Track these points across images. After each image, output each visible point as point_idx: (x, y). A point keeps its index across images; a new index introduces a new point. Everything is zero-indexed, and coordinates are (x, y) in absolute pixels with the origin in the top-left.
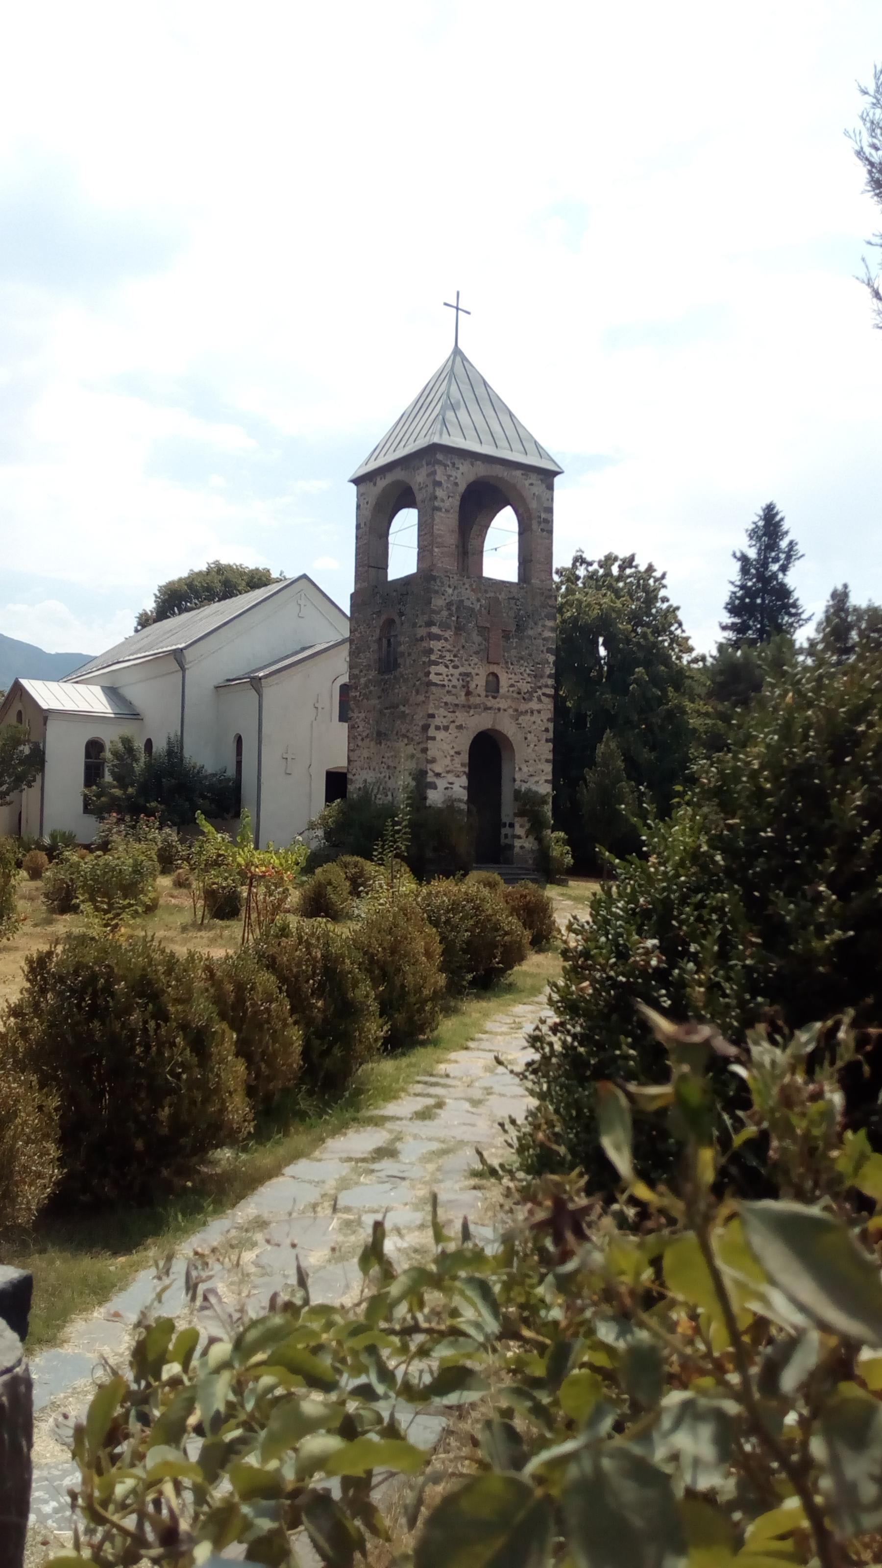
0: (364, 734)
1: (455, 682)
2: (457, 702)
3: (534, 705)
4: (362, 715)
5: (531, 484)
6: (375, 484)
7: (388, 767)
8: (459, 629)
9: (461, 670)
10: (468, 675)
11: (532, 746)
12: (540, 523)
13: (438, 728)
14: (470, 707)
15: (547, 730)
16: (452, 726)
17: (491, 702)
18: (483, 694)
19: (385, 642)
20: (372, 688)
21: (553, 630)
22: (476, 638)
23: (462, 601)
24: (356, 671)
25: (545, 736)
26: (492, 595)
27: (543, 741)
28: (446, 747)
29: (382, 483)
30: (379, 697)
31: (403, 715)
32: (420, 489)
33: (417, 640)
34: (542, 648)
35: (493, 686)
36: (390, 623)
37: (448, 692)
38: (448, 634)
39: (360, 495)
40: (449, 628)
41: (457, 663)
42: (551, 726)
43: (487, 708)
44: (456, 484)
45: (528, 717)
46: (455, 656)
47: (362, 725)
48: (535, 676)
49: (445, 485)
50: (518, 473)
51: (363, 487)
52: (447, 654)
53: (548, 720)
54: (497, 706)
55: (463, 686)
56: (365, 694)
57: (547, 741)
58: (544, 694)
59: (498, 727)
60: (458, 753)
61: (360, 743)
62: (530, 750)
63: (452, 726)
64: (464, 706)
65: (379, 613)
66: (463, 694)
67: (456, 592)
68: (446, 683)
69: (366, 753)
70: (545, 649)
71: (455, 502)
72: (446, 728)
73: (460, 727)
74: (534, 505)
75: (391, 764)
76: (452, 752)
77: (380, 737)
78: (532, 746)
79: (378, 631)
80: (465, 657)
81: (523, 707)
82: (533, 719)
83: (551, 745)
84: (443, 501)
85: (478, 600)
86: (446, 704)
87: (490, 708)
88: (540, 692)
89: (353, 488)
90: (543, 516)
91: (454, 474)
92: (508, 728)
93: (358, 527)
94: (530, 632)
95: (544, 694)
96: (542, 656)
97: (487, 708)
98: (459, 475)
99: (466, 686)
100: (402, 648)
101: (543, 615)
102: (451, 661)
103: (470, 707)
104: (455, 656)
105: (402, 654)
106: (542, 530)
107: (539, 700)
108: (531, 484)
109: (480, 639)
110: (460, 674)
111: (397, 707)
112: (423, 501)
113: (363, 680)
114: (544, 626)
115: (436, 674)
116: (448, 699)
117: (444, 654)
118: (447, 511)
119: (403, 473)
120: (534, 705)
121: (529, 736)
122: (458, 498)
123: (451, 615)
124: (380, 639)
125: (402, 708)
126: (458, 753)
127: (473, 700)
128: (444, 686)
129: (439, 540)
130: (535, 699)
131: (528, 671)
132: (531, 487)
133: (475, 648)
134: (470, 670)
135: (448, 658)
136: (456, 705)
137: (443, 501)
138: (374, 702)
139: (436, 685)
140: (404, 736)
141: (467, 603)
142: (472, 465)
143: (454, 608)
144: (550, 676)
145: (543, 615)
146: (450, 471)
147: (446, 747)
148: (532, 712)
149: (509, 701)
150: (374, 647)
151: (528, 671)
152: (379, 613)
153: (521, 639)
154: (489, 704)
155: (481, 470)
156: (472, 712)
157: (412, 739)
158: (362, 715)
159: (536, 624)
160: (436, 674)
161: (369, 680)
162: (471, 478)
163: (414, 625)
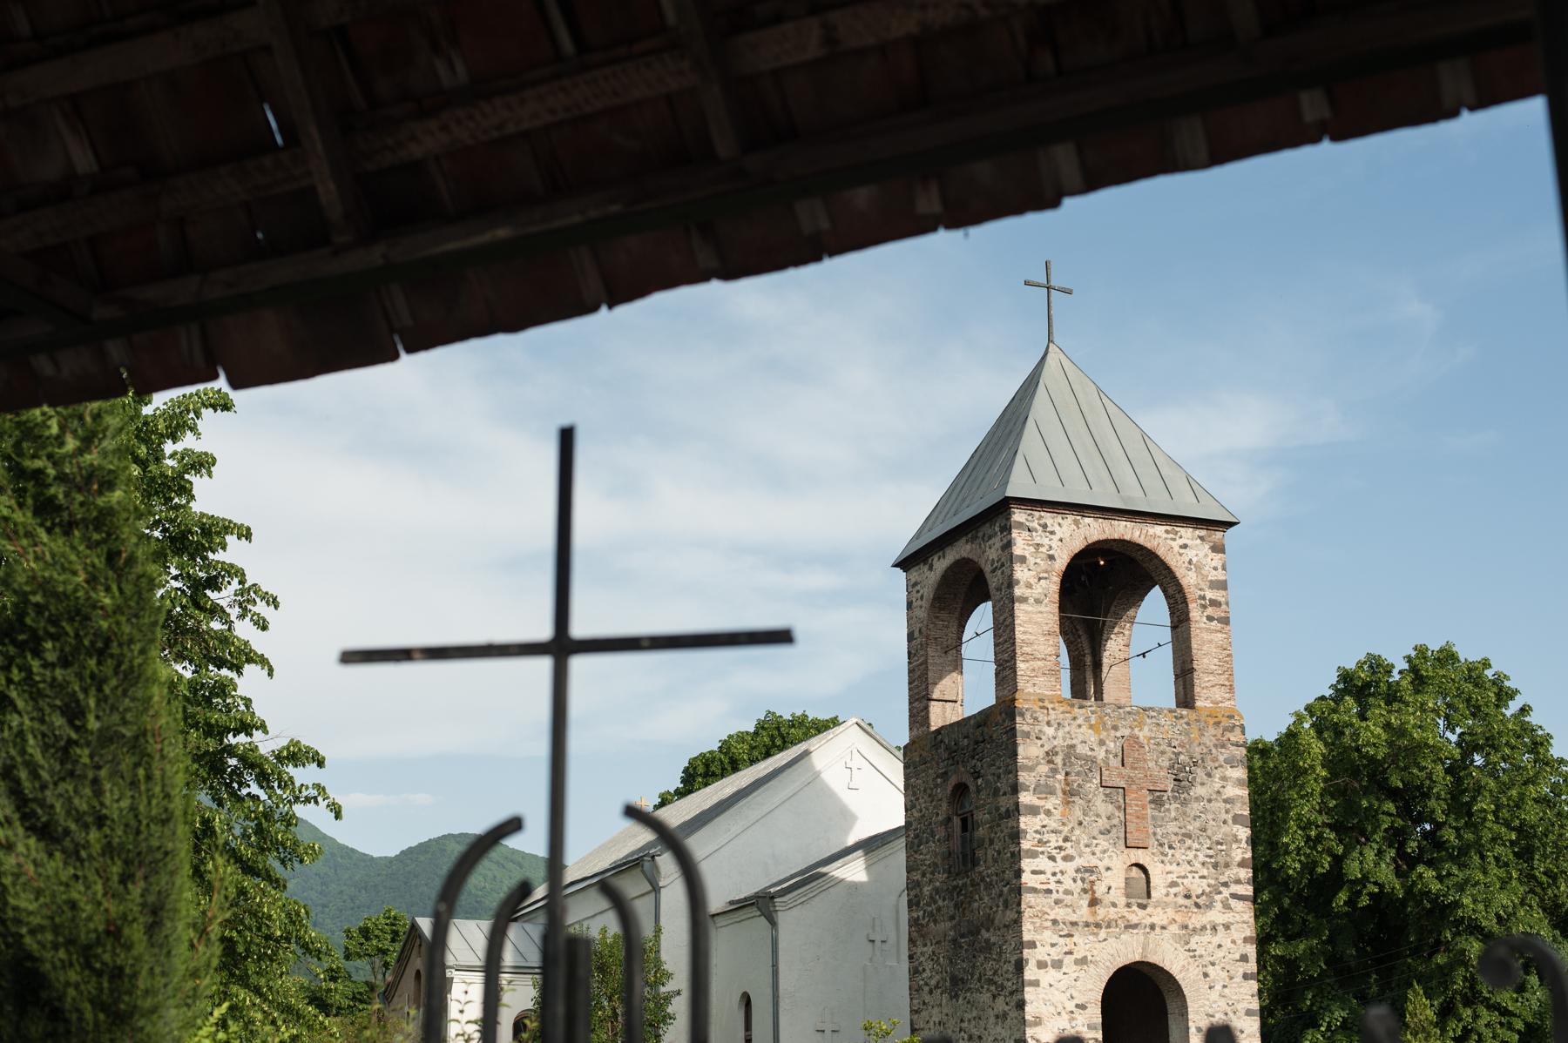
0: (933, 982)
1: (1068, 883)
2: (1074, 918)
3: (1216, 915)
4: (929, 949)
5: (1185, 546)
6: (931, 568)
8: (1070, 794)
9: (1079, 862)
10: (1090, 870)
11: (1218, 987)
12: (1204, 607)
13: (1041, 965)
14: (1098, 926)
15: (1244, 958)
16: (1068, 960)
17: (1136, 915)
18: (1122, 901)
19: (957, 821)
20: (940, 903)
21: (1239, 782)
22: (1101, 806)
23: (1073, 747)
24: (917, 876)
25: (1242, 968)
26: (1127, 732)
27: (1238, 979)
28: (1059, 997)
29: (941, 564)
30: (952, 918)
31: (988, 946)
32: (993, 571)
34: (1224, 816)
35: (1141, 886)
36: (961, 790)
37: (1057, 902)
38: (1052, 803)
39: (912, 586)
40: (1052, 792)
41: (1070, 851)
42: (1251, 950)
43: (1130, 926)
44: (1051, 558)
45: (1207, 937)
46: (1066, 840)
47: (928, 965)
48: (1215, 866)
49: (1031, 560)
50: (1159, 530)
51: (915, 575)
52: (1053, 838)
53: (1246, 940)
54: (1148, 921)
55: (1085, 891)
56: (931, 914)
57: (1246, 977)
58: (1234, 896)
59: (1153, 959)
60: (1082, 1007)
61: (927, 998)
62: (1214, 995)
63: (1068, 960)
64: (1087, 925)
65: (945, 776)
66: (1085, 903)
67: (1060, 733)
68: (1052, 886)
70: (1229, 817)
71: (1053, 586)
72: (1058, 964)
73: (1082, 961)
74: (1188, 579)
75: (975, 1032)
76: (1071, 1006)
77: (956, 985)
78: (1218, 987)
79: (945, 805)
80: (1085, 839)
81: (1197, 920)
82: (1216, 940)
83: (1253, 986)
84: (1029, 586)
85: (1102, 743)
86: (1055, 922)
87: (1135, 926)
88: (1226, 892)
89: (901, 575)
90: (1210, 594)
91: (1046, 541)
92: (1172, 959)
93: (910, 637)
94: (1198, 791)
95: (1234, 896)
96: (1225, 829)
97: (1130, 926)
98: (1055, 544)
99: (1089, 890)
100: (981, 832)
101: (1221, 758)
102: (1060, 848)
103: (1098, 926)
104: (1066, 840)
105: (981, 844)
106: (1210, 619)
107: (1227, 907)
108: (1185, 546)
109: (1110, 807)
110: (1077, 871)
111: (978, 932)
112: (999, 589)
113: (927, 890)
114: (1224, 778)
115: (1034, 872)
116: (1060, 913)
117: (1046, 837)
118: (1038, 601)
119: (968, 547)
120: (1216, 915)
121: (1210, 970)
122: (1057, 580)
123: (1055, 771)
124: (949, 819)
125: (985, 934)
126: (1082, 1007)
127: (1101, 912)
128: (1049, 891)
129: (1027, 649)
130: (1219, 905)
131: (1201, 858)
132: (1184, 553)
133: (1103, 823)
134: (1094, 861)
135: (1053, 844)
136: (1074, 924)
137: (1029, 586)
138: (945, 926)
139: (1034, 890)
140: (991, 982)
141: (1082, 750)
142: (1077, 523)
143: (1059, 760)
144: (1242, 864)
145: (1221, 758)
146: (1039, 537)
147: (1059, 997)
148: (1214, 928)
149: (1171, 913)
150: (941, 833)
151: (1201, 858)
152: (945, 776)
153: (1184, 803)
154: (1134, 919)
155: (1096, 530)
156: (1103, 934)
157: (1003, 987)
158: (929, 949)
159: (1209, 775)
160: (1034, 872)
161: (937, 890)
162: (1078, 545)
163: (996, 792)
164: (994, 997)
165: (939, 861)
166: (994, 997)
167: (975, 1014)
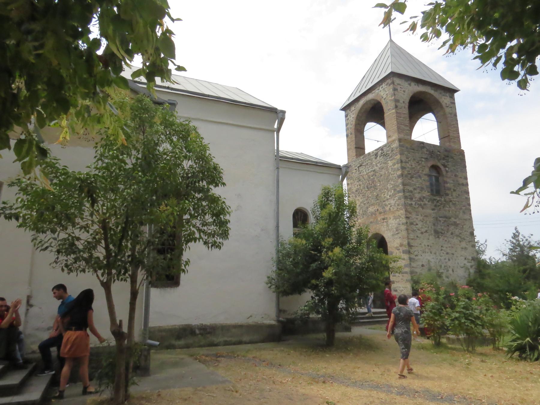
0: (423, 230)
7: (447, 253)
20: (427, 203)
33: (459, 184)
61: (420, 235)
69: (425, 242)
75: (448, 251)
105: (449, 189)
111: (450, 218)
113: (417, 196)
158: (420, 218)
161: (424, 198)
164: (460, 242)
165: (425, 187)
166: (460, 242)
167: (450, 245)
